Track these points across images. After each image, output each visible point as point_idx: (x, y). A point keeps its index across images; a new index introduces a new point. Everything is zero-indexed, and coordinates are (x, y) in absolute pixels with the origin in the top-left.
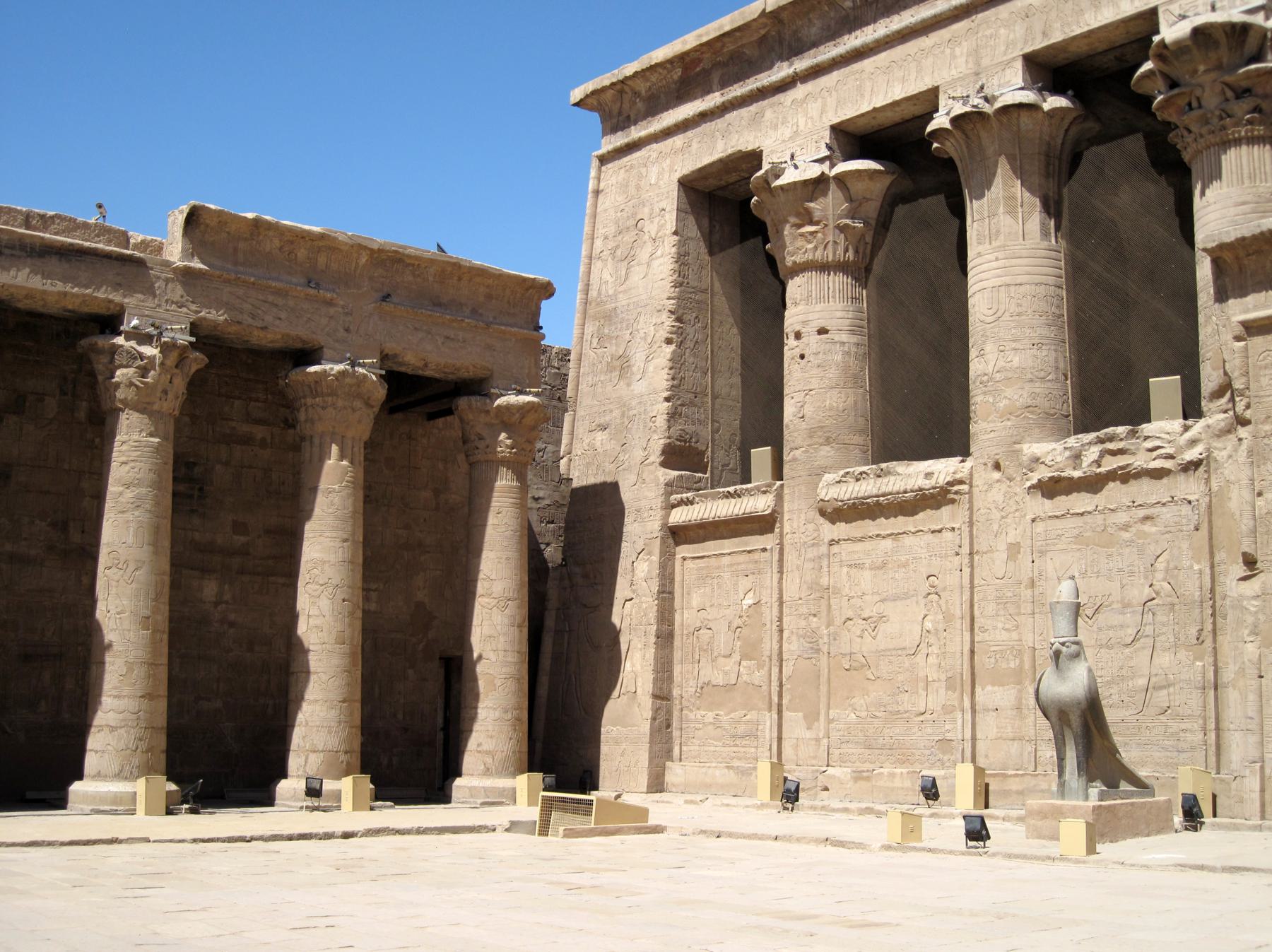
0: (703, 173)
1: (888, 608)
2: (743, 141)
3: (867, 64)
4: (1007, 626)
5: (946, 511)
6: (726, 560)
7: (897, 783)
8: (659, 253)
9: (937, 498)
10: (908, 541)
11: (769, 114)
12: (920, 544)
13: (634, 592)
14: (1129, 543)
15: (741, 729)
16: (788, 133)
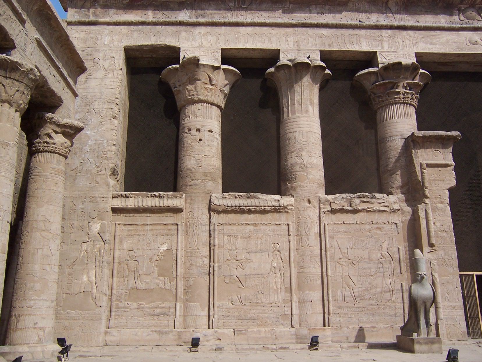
0: (140, 49)
1: (252, 256)
2: (172, 42)
3: (242, 29)
5: (283, 216)
6: (148, 228)
7: (263, 335)
8: (110, 75)
9: (277, 210)
10: (262, 227)
11: (184, 34)
12: (270, 228)
13: (89, 238)
14: (371, 237)
15: (158, 311)
16: (197, 45)
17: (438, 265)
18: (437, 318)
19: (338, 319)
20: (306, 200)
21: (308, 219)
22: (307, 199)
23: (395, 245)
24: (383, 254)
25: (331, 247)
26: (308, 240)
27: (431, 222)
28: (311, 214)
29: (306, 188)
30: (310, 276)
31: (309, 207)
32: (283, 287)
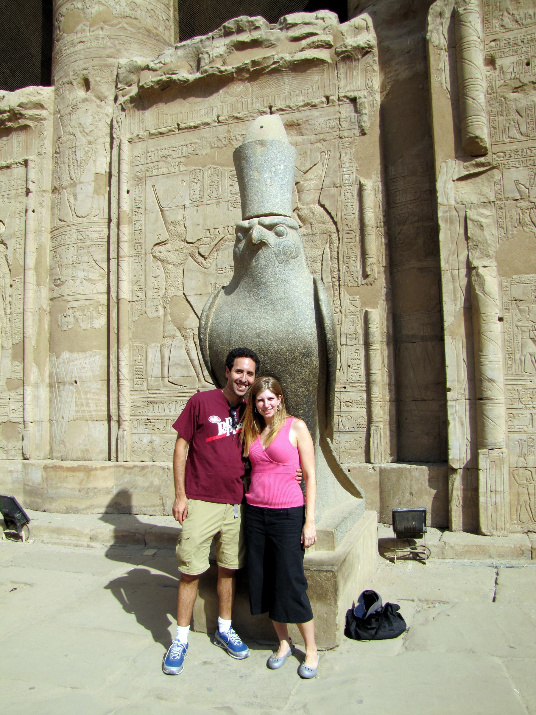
4: (91, 275)
17: (499, 226)
18: (478, 439)
19: (146, 439)
20: (77, 82)
21: (79, 135)
22: (80, 80)
23: (349, 177)
24: (305, 212)
25: (136, 209)
26: (76, 199)
27: (476, 57)
28: (87, 120)
29: (80, 47)
30: (76, 304)
31: (85, 100)
32: (9, 344)
